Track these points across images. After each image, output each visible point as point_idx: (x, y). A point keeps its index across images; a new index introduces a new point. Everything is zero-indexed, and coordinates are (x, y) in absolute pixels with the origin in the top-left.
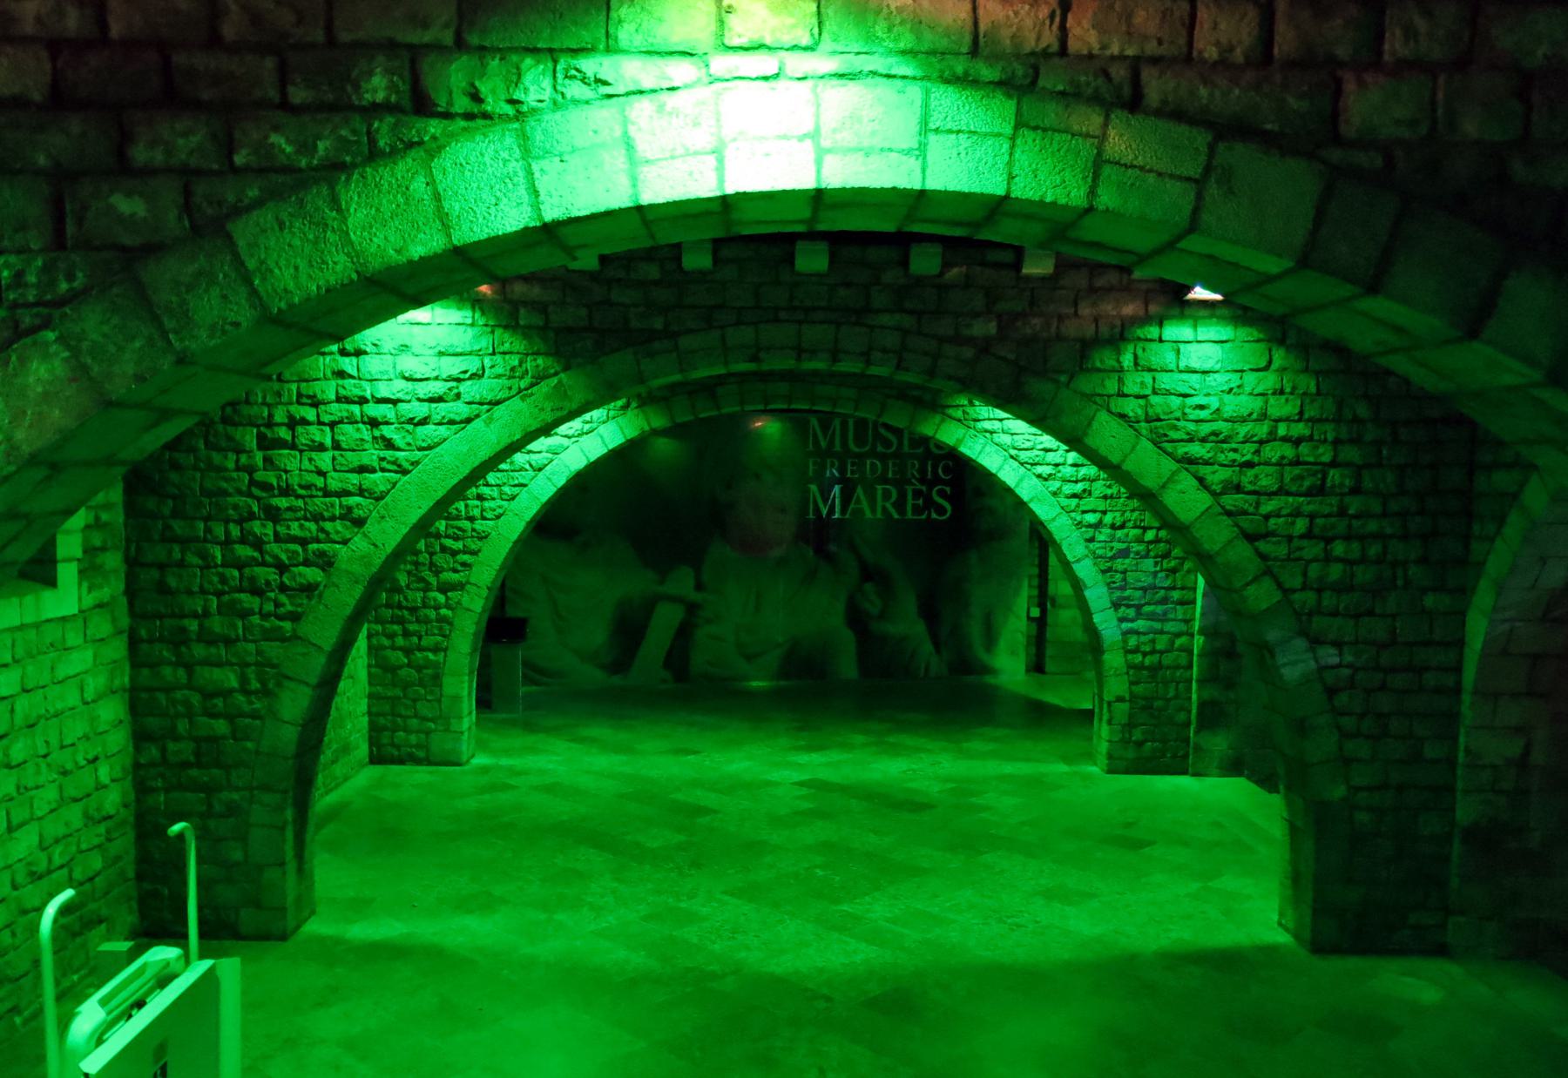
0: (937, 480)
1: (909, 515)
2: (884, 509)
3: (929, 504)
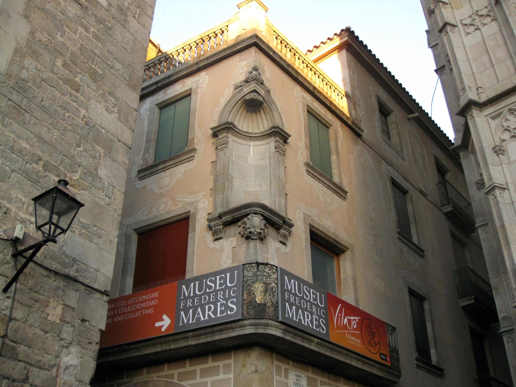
0: (230, 297)
2: (209, 315)
3: (227, 308)
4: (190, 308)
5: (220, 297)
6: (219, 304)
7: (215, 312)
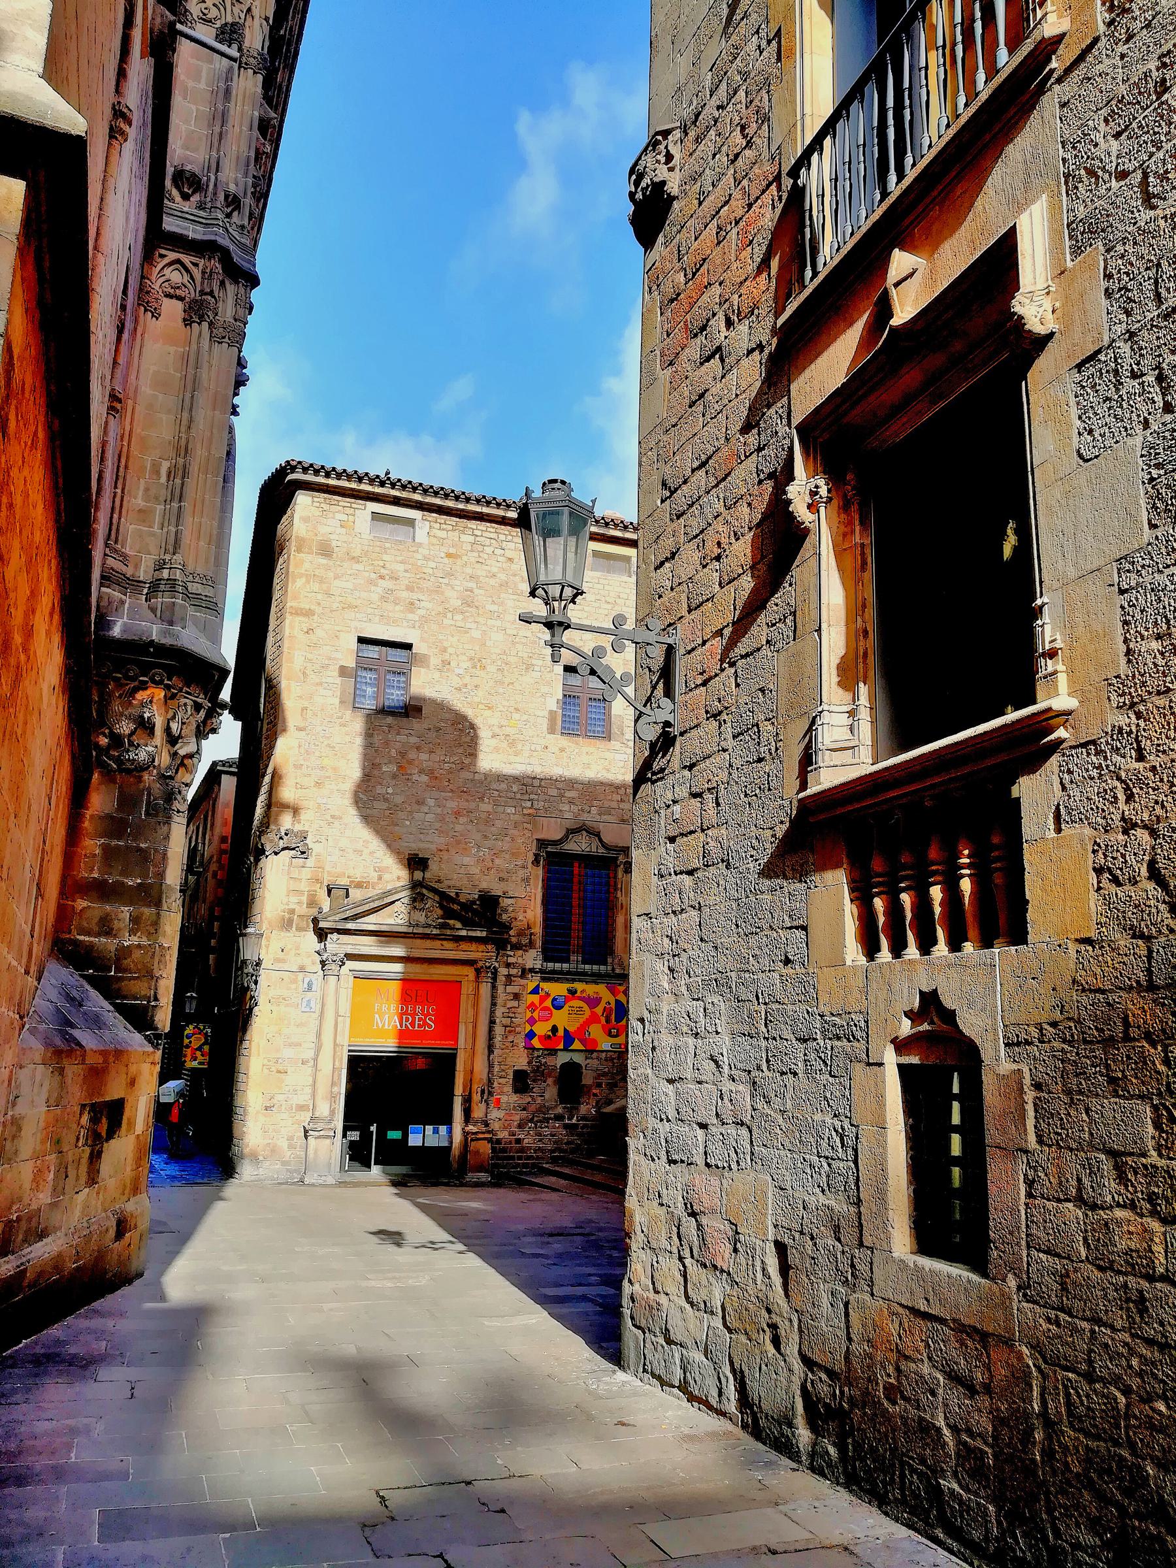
3: (425, 1023)
7: (413, 1024)
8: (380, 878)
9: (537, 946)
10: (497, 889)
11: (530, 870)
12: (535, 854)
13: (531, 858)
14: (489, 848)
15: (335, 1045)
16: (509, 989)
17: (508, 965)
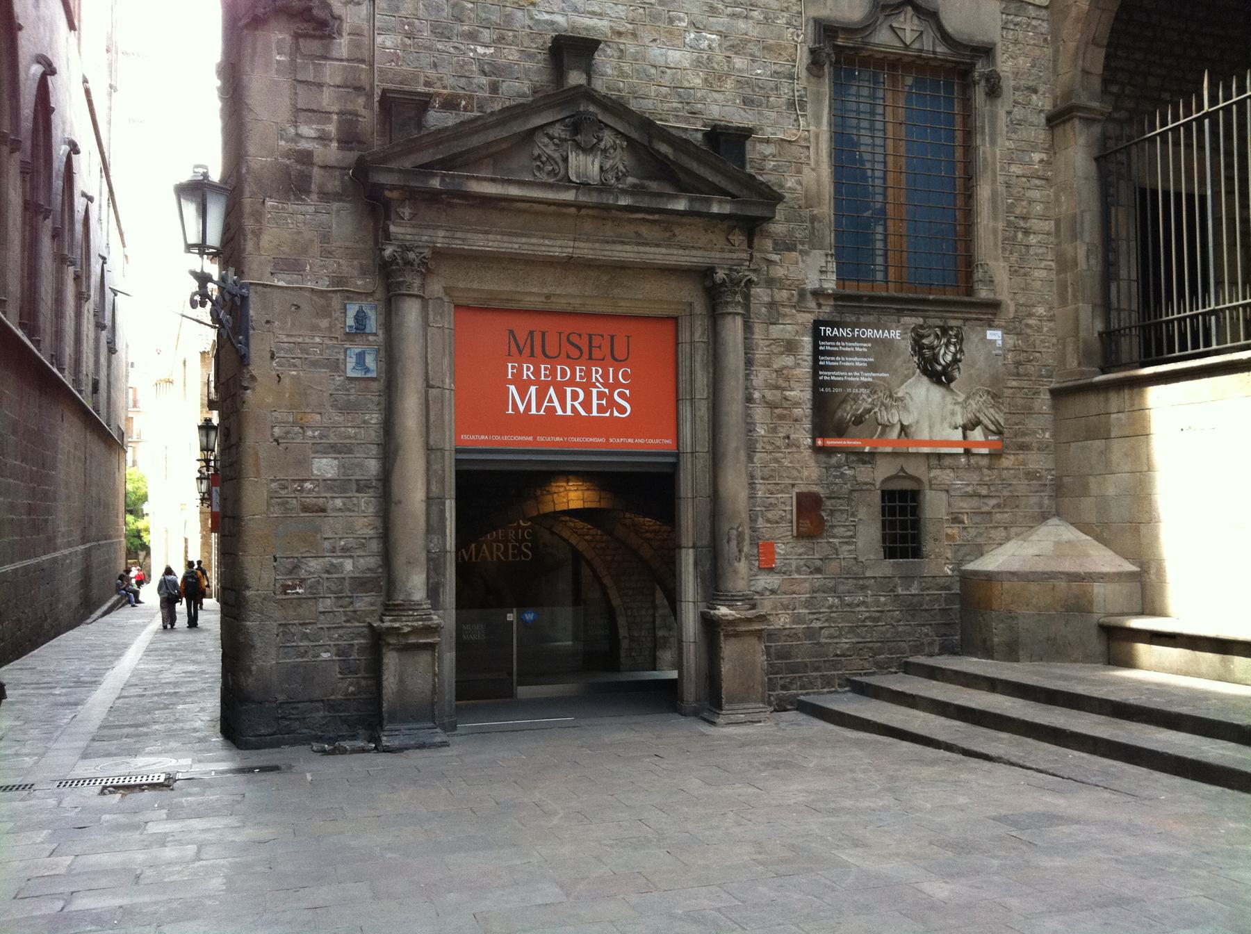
0: (617, 384)
1: (595, 413)
2: (574, 408)
3: (612, 403)
4: (530, 382)
5: (596, 378)
6: (594, 391)
7: (587, 404)
8: (494, 88)
9: (827, 241)
10: (739, 117)
11: (805, 84)
12: (813, 52)
13: (803, 58)
14: (719, 33)
15: (429, 449)
16: (775, 331)
17: (770, 283)
